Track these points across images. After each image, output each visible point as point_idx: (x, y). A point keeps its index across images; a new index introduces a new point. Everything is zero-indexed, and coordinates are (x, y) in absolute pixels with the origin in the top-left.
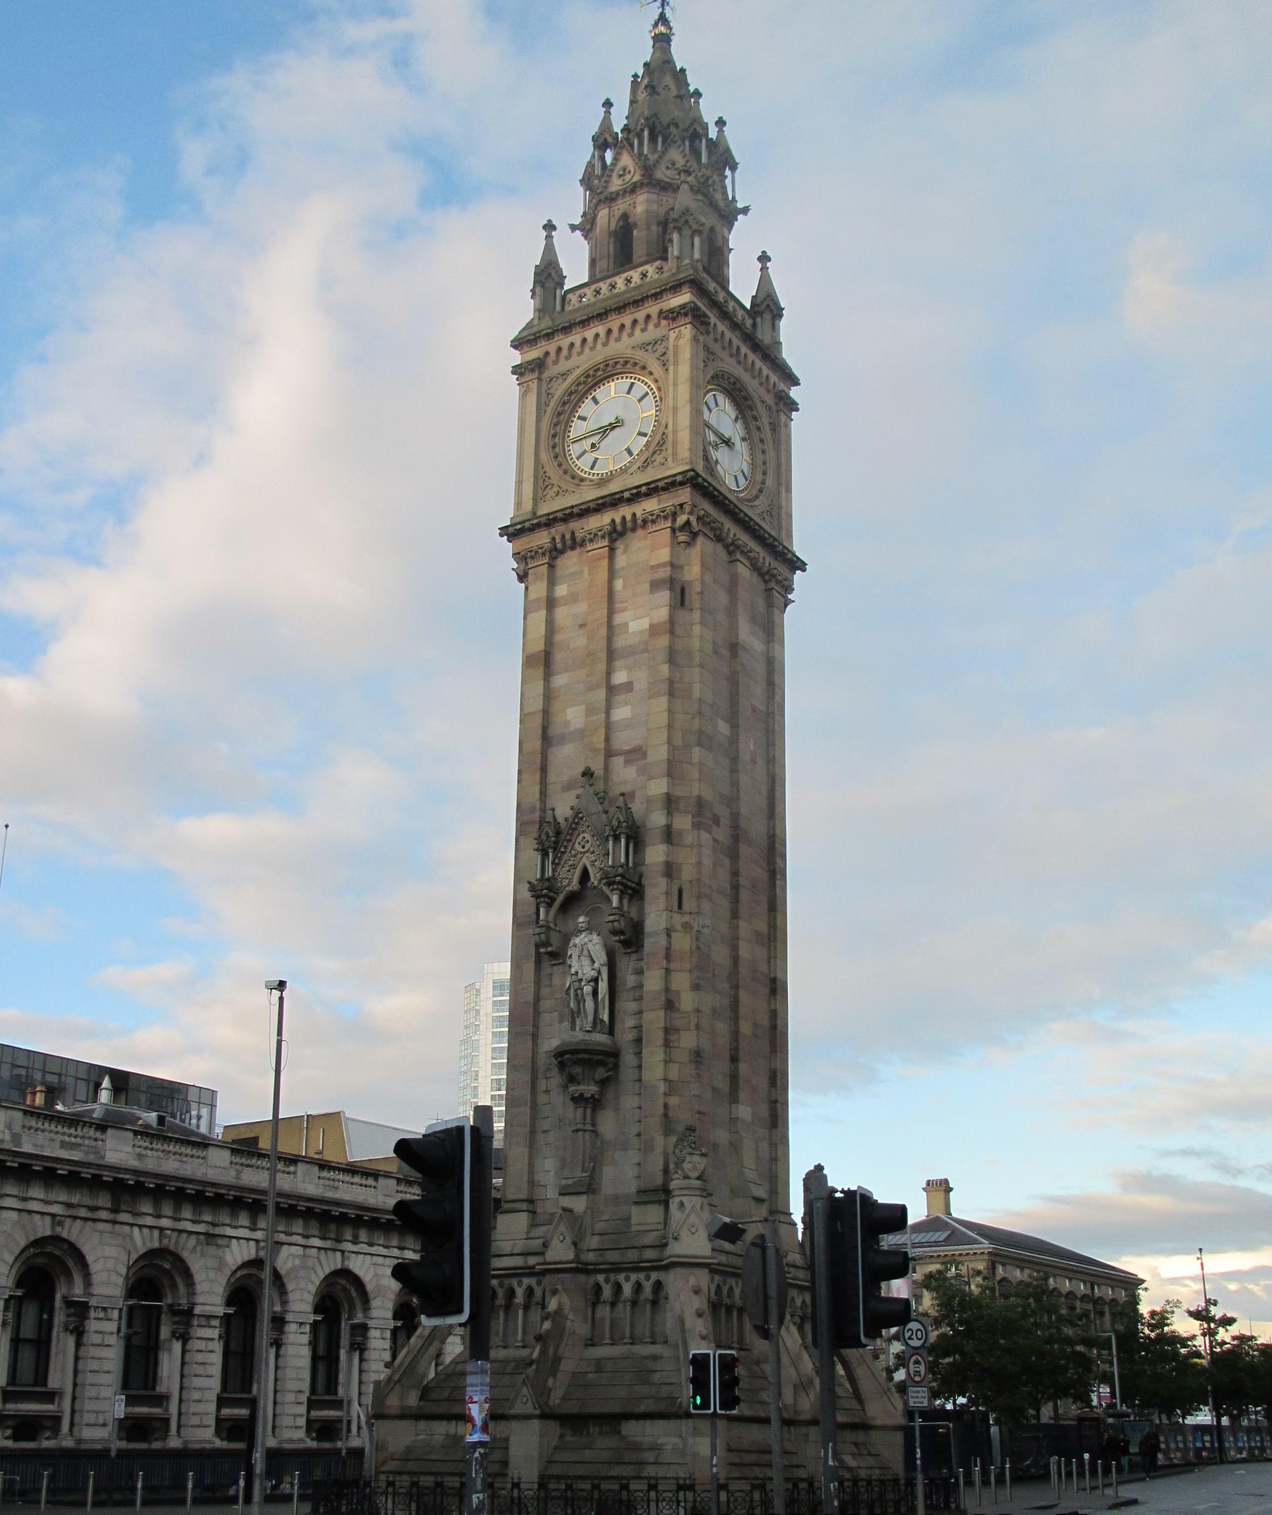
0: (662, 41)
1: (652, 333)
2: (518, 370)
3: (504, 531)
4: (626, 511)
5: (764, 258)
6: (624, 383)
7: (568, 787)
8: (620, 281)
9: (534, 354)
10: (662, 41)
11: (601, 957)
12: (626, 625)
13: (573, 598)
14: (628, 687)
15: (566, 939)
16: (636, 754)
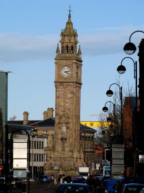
0: (70, 16)
1: (71, 63)
2: (55, 63)
3: (54, 82)
4: (68, 84)
5: (80, 46)
6: (67, 67)
7: (62, 111)
8: (67, 54)
9: (57, 61)
10: (70, 16)
11: (66, 130)
12: (68, 96)
13: (62, 91)
14: (68, 102)
15: (62, 127)
16: (69, 109)
